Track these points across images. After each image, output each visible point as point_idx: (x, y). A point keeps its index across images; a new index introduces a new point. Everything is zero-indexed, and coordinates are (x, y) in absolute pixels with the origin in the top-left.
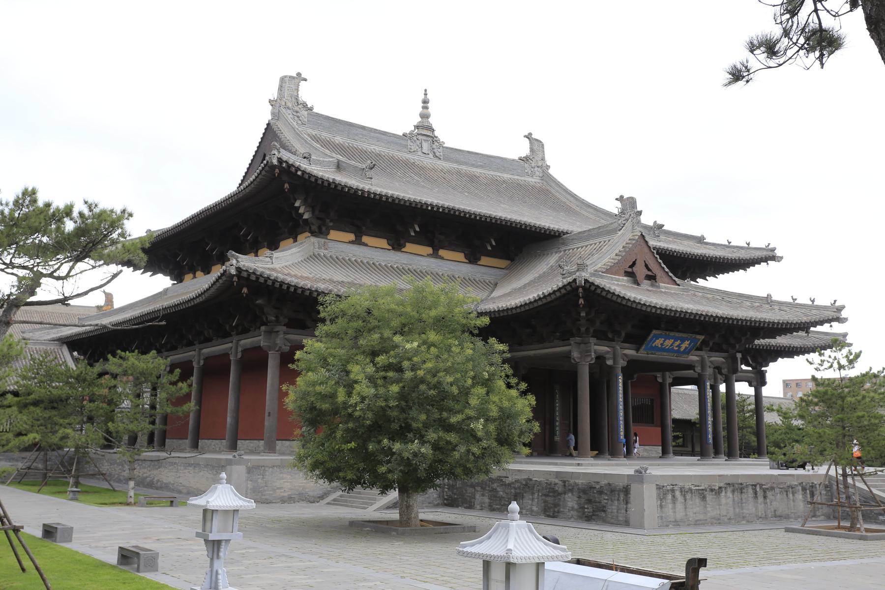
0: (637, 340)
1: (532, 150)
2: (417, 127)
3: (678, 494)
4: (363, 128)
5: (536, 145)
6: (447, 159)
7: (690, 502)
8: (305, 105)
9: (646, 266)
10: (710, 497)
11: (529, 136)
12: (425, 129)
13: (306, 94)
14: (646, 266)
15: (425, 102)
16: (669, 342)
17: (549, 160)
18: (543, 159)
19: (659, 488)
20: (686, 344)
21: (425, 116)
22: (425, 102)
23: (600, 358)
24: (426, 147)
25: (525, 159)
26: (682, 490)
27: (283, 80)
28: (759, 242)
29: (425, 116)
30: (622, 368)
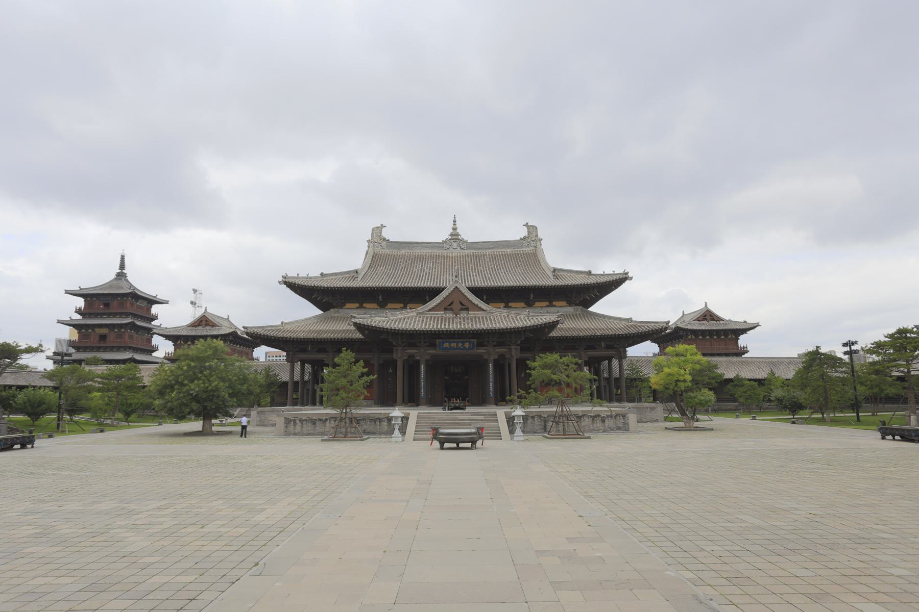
0: (433, 345)
1: (529, 232)
2: (452, 235)
3: (298, 421)
4: (417, 243)
5: (532, 229)
6: (468, 249)
7: (305, 425)
8: (385, 239)
9: (461, 304)
10: (318, 423)
11: (526, 225)
12: (455, 236)
13: (386, 234)
14: (461, 304)
15: (455, 221)
16: (454, 345)
17: (540, 236)
18: (537, 236)
19: (286, 419)
20: (467, 345)
21: (454, 229)
22: (455, 221)
23: (411, 356)
24: (455, 245)
25: (525, 238)
26: (300, 420)
27: (373, 230)
28: (619, 270)
29: (454, 229)
30: (427, 360)
